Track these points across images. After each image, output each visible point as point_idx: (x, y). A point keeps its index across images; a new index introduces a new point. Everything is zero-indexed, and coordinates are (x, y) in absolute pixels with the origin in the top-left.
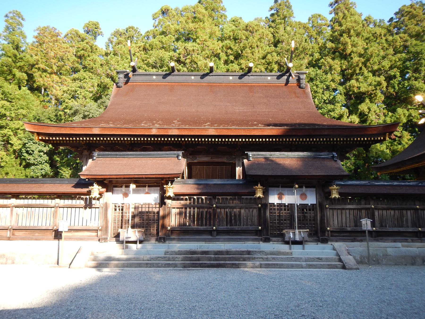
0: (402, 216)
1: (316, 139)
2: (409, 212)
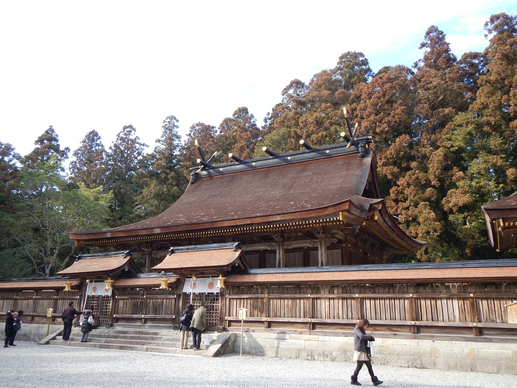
0: (294, 306)
1: (273, 226)
2: (302, 301)
